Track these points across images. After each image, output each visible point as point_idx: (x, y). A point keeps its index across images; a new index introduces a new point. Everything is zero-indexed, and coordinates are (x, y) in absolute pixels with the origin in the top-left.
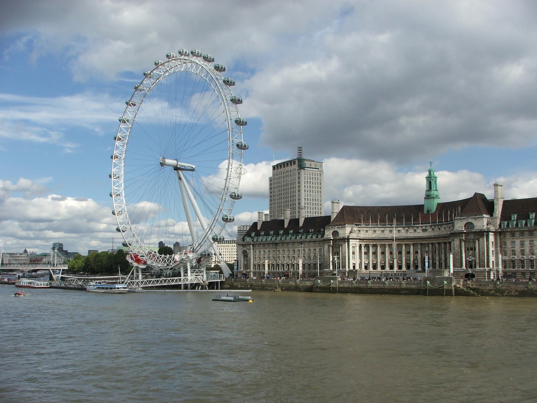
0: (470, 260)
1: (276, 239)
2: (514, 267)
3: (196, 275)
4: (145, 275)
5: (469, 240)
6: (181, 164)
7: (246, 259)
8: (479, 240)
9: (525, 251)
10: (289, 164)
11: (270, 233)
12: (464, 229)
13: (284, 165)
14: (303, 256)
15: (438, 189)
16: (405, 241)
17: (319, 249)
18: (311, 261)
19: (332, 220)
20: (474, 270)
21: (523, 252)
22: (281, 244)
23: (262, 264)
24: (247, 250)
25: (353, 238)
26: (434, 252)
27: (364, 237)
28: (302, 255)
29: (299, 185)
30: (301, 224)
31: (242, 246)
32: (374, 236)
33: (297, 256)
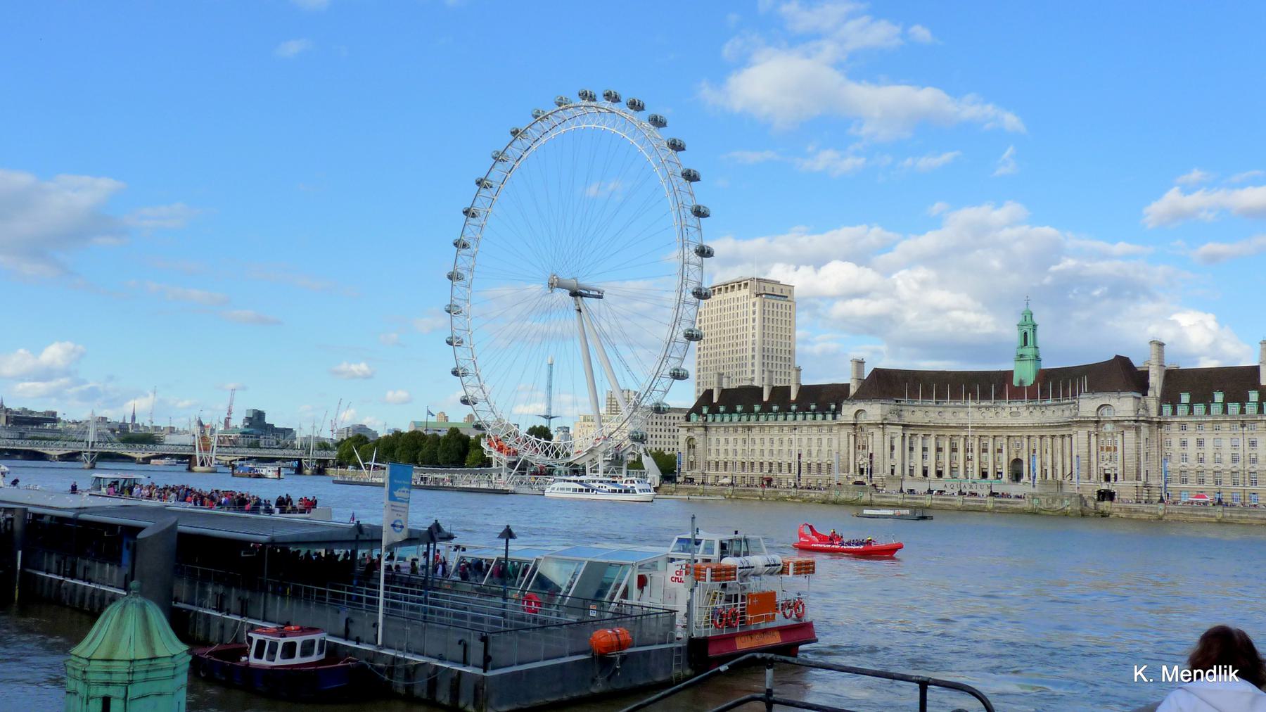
0: (1107, 467)
1: (749, 420)
7: (692, 452)
15: (1038, 345)
19: (852, 391)
22: (758, 428)
24: (695, 437)
28: (797, 449)
30: (793, 397)
31: (686, 429)
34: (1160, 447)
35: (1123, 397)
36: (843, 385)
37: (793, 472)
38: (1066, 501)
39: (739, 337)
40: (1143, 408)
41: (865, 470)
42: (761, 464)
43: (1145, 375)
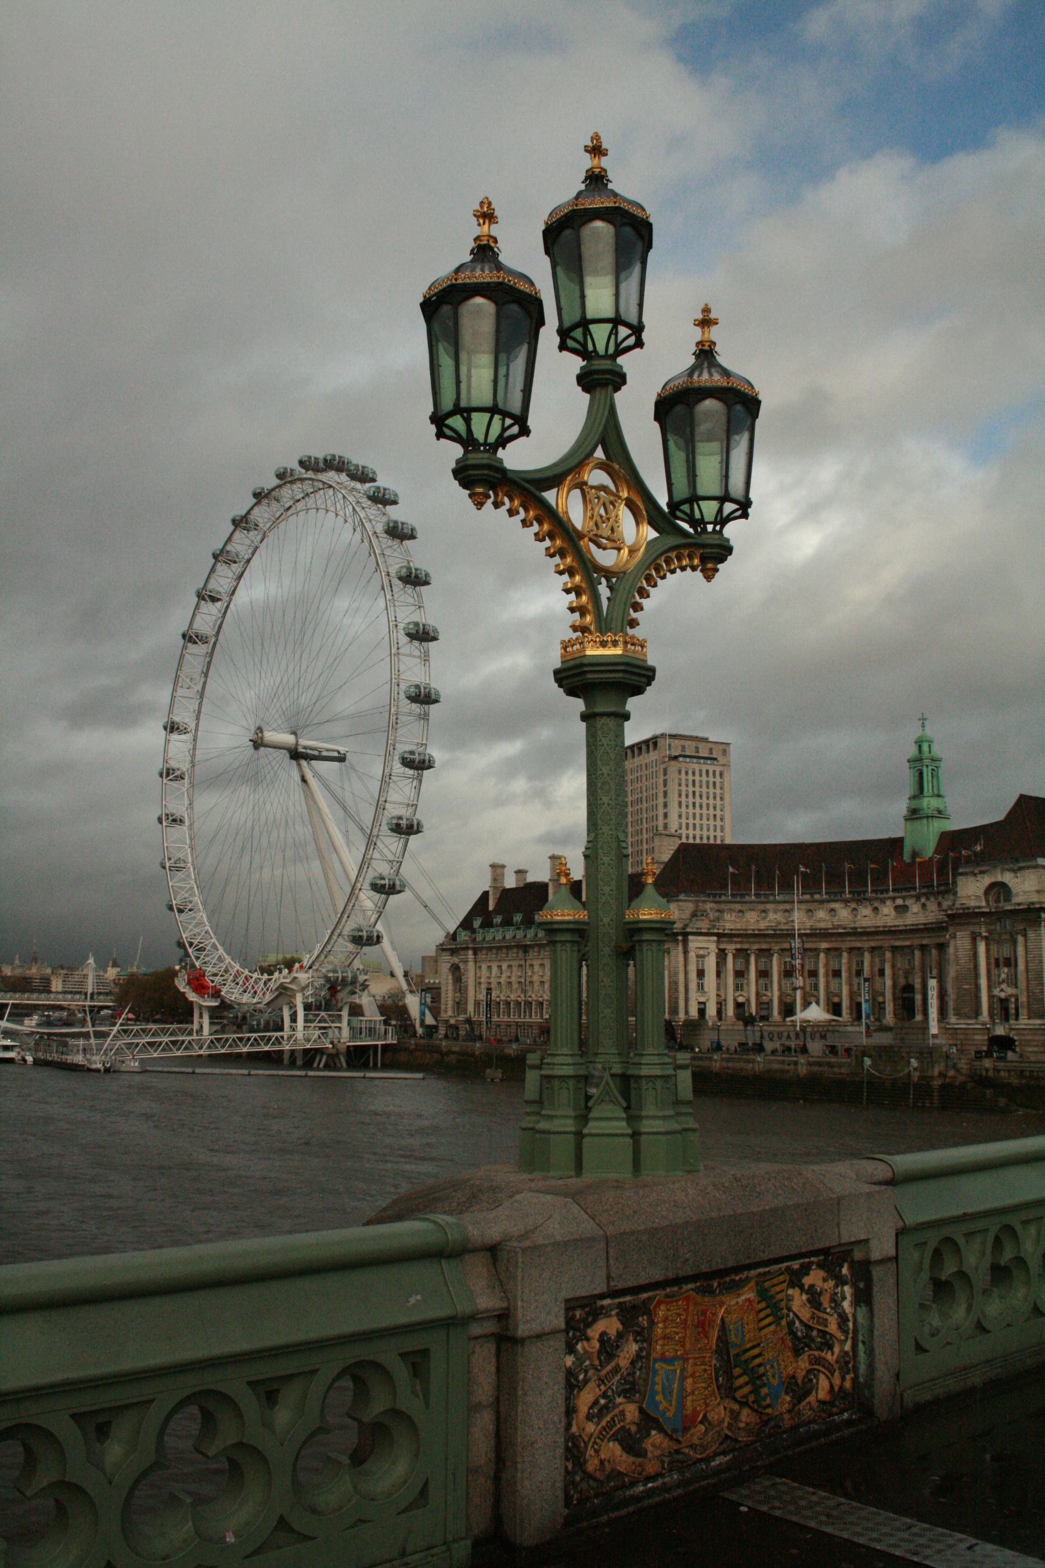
0: (1003, 995)
1: (525, 936)
4: (221, 1023)
6: (303, 742)
7: (458, 988)
8: (1025, 935)
10: (644, 747)
11: (515, 919)
12: (984, 904)
13: (633, 752)
16: (851, 941)
20: (1013, 1027)
24: (462, 966)
27: (732, 930)
31: (448, 953)
32: (763, 925)
38: (912, 1060)
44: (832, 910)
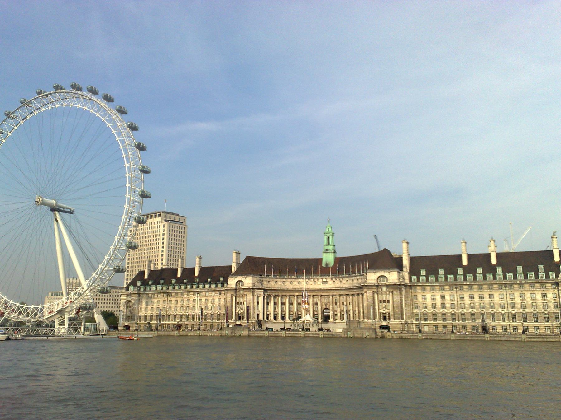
0: (384, 312)
1: (168, 289)
2: (435, 320)
3: (74, 328)
5: (382, 292)
9: (437, 305)
14: (199, 306)
17: (218, 299)
18: (208, 312)
19: (234, 270)
21: (434, 307)
22: (173, 294)
23: (148, 315)
25: (259, 288)
26: (349, 304)
28: (198, 306)
29: (164, 237)
30: (197, 274)
31: (126, 295)
33: (192, 307)
34: (412, 300)
35: (392, 272)
36: (227, 266)
37: (195, 320)
39: (154, 244)
40: (402, 278)
41: (242, 317)
42: (175, 316)
43: (400, 259)
44: (300, 282)
